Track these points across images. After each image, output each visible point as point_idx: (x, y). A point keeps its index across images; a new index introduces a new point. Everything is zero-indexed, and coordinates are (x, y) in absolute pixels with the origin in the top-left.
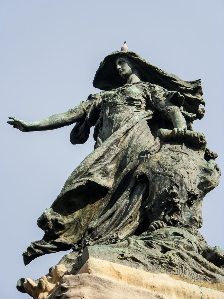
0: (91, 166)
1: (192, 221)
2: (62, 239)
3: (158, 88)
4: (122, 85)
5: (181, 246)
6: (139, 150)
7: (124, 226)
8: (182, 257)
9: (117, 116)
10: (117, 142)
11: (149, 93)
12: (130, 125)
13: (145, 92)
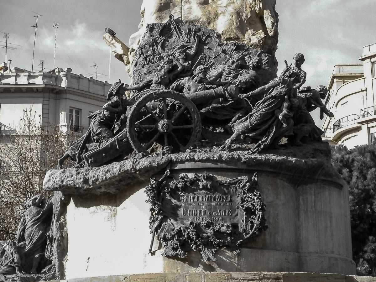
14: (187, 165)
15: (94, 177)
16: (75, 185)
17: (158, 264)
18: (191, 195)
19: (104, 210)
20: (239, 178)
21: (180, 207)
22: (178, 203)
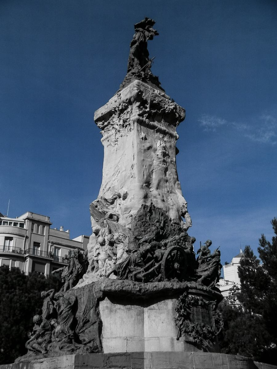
14: (194, 291)
15: (146, 288)
16: (131, 291)
17: (180, 346)
18: (195, 308)
19: (137, 308)
20: (211, 302)
21: (191, 314)
22: (190, 311)
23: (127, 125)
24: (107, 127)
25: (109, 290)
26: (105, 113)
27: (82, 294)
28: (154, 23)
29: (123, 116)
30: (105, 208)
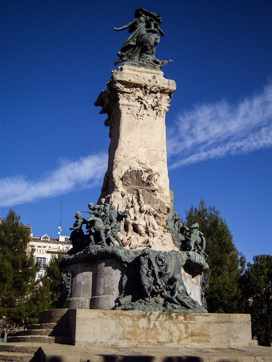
0: (130, 40)
1: (153, 52)
2: (124, 59)
3: (148, 17)
4: (139, 17)
5: (147, 60)
6: (142, 34)
7: (136, 55)
8: (147, 63)
9: (137, 26)
10: (136, 33)
11: (146, 19)
12: (140, 28)
13: (145, 19)
23: (158, 109)
24: (128, 94)
25: (200, 263)
26: (134, 82)
27: (170, 259)
28: (160, 22)
29: (151, 97)
30: (153, 180)
